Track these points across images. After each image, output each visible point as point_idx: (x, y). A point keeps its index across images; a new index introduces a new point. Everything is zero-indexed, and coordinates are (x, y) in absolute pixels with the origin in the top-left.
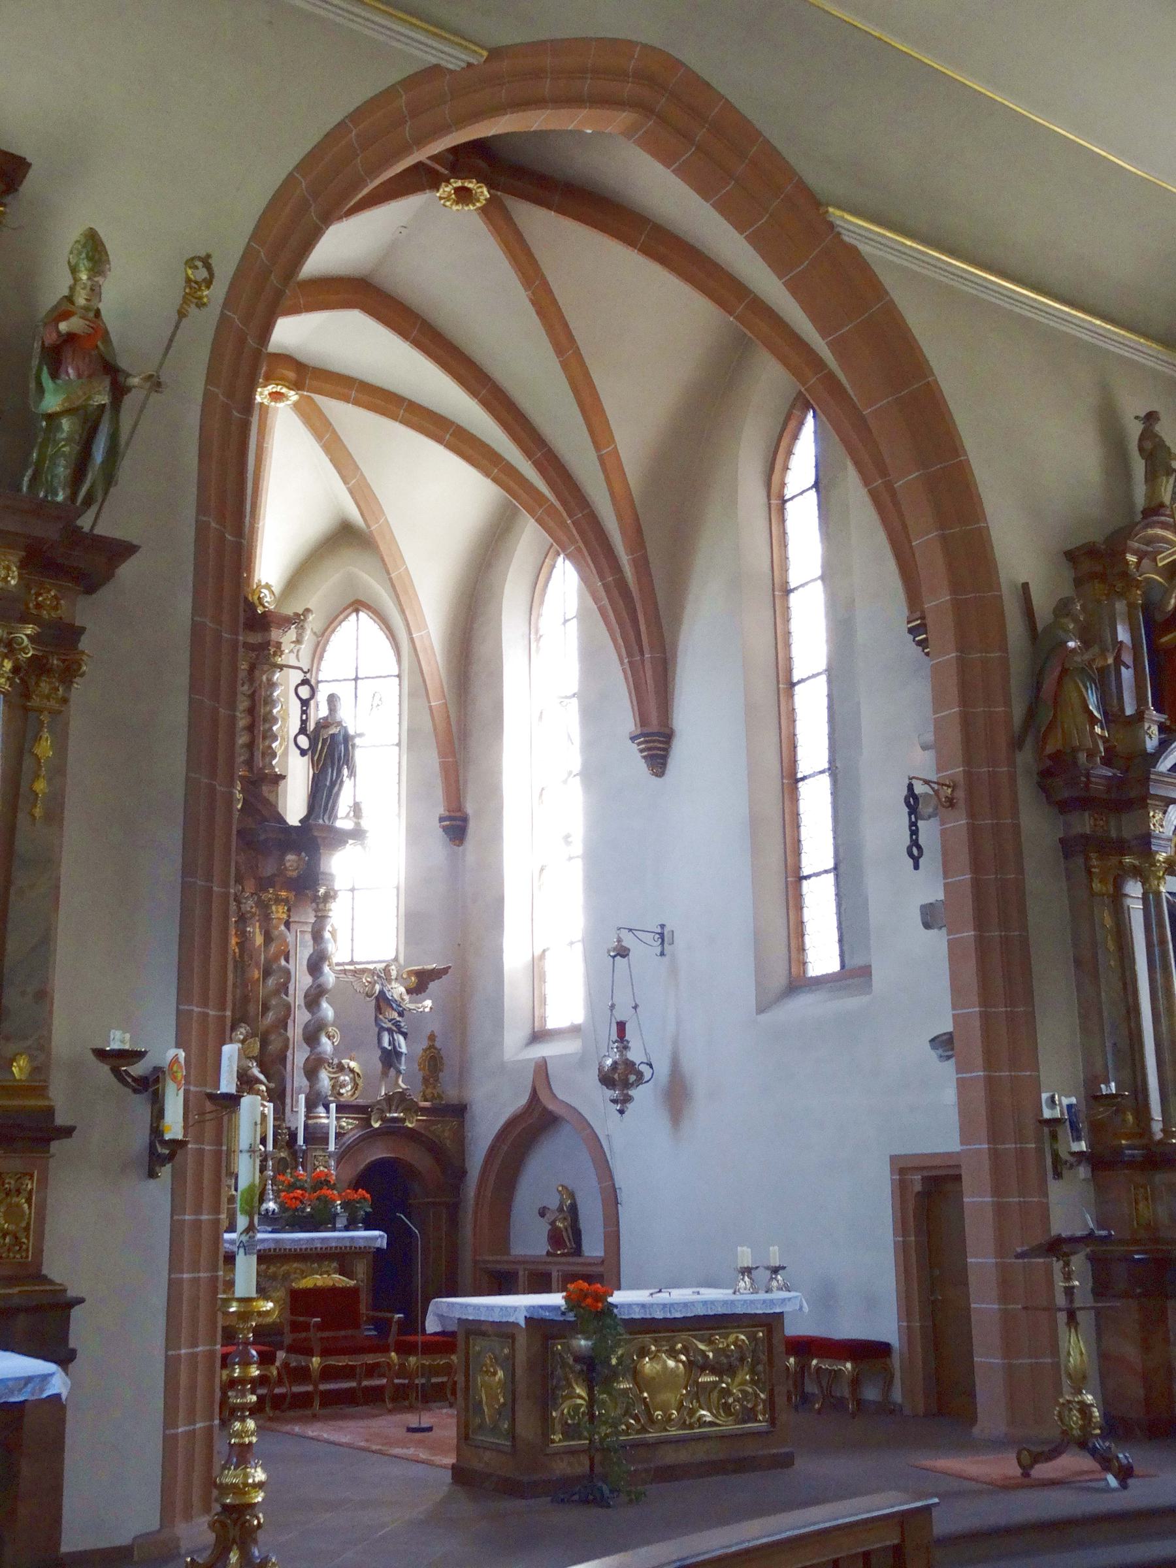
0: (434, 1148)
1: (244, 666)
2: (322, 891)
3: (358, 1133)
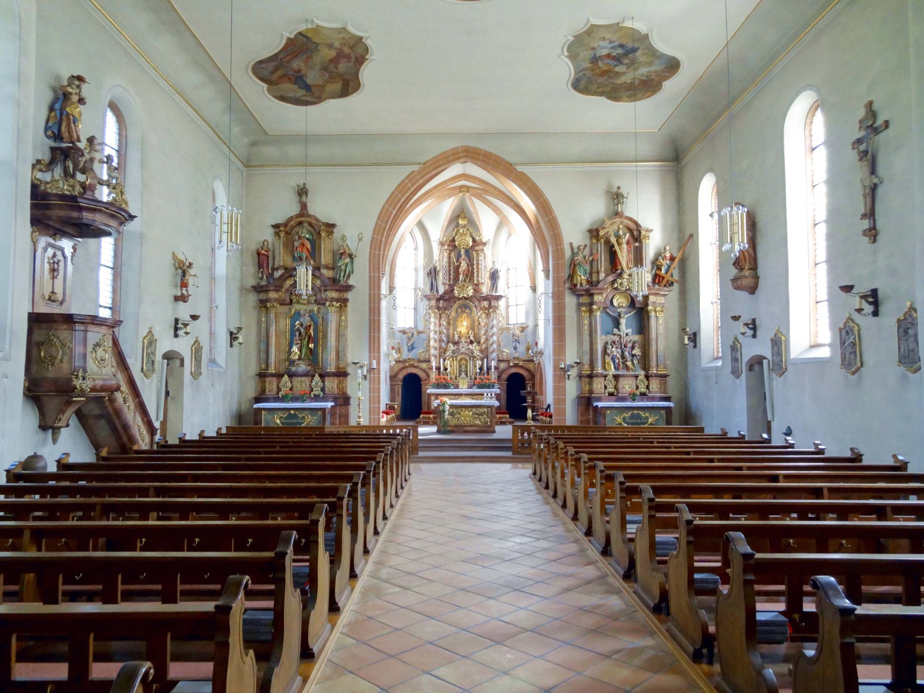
0: (528, 370)
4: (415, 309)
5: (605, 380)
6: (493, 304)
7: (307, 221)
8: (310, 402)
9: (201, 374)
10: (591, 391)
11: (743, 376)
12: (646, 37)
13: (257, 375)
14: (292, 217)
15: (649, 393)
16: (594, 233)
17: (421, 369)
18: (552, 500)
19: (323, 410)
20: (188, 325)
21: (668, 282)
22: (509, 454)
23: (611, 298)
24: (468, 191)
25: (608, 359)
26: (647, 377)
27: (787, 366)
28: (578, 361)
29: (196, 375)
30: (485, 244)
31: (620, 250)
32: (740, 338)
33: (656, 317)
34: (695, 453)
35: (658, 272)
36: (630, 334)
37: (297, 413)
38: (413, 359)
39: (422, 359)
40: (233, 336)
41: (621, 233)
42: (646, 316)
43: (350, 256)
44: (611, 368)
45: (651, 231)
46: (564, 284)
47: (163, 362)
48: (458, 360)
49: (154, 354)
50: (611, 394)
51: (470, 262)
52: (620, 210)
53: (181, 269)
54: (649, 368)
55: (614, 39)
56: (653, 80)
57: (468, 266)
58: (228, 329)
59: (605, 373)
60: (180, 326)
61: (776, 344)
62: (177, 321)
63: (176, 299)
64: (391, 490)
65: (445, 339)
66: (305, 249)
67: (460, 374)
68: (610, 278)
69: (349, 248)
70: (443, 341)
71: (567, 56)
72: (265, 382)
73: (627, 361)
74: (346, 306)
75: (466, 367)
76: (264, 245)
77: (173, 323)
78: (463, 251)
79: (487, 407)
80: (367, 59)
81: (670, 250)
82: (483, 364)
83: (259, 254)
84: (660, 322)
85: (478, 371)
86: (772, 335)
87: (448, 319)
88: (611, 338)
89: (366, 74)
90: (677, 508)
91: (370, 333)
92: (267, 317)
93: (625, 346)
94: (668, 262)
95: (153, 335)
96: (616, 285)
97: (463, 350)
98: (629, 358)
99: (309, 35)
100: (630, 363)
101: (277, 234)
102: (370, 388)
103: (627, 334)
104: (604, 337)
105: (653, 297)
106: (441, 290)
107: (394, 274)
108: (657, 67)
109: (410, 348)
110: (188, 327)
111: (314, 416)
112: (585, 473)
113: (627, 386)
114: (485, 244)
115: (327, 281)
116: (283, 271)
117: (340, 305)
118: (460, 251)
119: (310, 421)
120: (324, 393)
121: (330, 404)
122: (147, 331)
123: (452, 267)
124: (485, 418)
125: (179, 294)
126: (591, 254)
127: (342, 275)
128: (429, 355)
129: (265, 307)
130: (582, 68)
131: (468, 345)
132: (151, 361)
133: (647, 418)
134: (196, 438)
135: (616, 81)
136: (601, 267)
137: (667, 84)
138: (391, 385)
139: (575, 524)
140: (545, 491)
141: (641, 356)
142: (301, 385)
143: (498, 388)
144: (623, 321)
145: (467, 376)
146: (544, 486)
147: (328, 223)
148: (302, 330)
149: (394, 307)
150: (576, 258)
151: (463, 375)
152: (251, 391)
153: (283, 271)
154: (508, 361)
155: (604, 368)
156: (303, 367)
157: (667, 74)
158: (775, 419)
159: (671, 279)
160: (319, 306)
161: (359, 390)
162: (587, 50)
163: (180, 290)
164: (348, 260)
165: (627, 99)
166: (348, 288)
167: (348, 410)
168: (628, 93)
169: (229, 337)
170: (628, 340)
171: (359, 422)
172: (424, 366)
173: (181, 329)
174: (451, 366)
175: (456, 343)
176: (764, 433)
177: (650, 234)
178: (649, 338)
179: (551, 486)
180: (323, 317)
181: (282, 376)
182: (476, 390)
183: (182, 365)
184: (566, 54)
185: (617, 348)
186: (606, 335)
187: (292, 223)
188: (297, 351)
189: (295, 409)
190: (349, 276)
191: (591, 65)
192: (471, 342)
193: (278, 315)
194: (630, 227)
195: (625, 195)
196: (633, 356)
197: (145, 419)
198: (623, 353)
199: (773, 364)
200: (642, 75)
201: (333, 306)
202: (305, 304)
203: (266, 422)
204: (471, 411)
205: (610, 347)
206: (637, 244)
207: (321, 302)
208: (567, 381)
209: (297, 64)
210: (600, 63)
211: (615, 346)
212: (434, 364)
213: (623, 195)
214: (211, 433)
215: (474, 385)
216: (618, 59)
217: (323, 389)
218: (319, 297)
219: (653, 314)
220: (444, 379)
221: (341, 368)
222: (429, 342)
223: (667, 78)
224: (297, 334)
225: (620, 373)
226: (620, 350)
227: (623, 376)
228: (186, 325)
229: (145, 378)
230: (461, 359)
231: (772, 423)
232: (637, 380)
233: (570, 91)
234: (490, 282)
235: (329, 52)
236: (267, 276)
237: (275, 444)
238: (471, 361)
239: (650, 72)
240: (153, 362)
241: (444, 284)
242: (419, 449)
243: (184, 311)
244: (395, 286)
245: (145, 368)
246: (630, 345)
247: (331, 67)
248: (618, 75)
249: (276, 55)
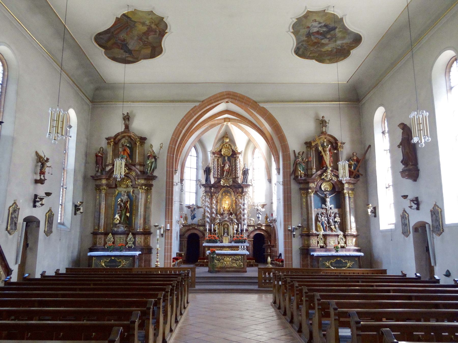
1: (234, 160)
2: (244, 194)
3: (253, 229)
4: (196, 193)
5: (318, 238)
6: (244, 190)
7: (128, 136)
8: (126, 251)
9: (52, 232)
10: (309, 245)
11: (411, 235)
12: (342, 19)
13: (91, 233)
14: (119, 133)
15: (347, 246)
16: (308, 144)
17: (199, 231)
18: (289, 325)
19: (133, 257)
20: (43, 199)
21: (355, 175)
22: (256, 287)
24: (229, 121)
25: (319, 224)
26: (345, 236)
27: (444, 229)
28: (300, 225)
29: (48, 233)
30: (240, 153)
31: (325, 155)
32: (408, 210)
34: (395, 291)
36: (333, 208)
37: (116, 259)
38: (194, 224)
39: (200, 224)
40: (77, 208)
41: (325, 144)
43: (155, 157)
44: (321, 230)
45: (344, 143)
47: (23, 224)
48: (222, 225)
49: (17, 218)
50: (322, 247)
51: (230, 164)
52: (324, 130)
53: (41, 162)
54: (346, 230)
55: (322, 21)
56: (344, 49)
57: (229, 167)
58: (73, 203)
59: (318, 233)
60: (38, 200)
61: (435, 214)
62: (36, 196)
63: (36, 182)
64: (171, 318)
65: (215, 212)
66: (125, 153)
67: (224, 234)
68: (319, 172)
69: (154, 152)
70: (213, 213)
71: (292, 32)
72: (96, 238)
73: (331, 225)
74: (151, 189)
75: (228, 229)
76: (100, 150)
77: (33, 197)
78: (226, 158)
79: (241, 255)
80: (167, 33)
81: (356, 155)
82: (238, 227)
83: (97, 156)
84: (352, 201)
85: (235, 232)
86: (431, 208)
87: (217, 199)
88: (321, 211)
89: (166, 42)
90: (382, 332)
91: (166, 206)
92: (100, 196)
93: (330, 216)
95: (17, 206)
96: (323, 177)
97: (226, 219)
98: (333, 224)
99: (130, 16)
100: (334, 227)
101: (109, 143)
102: (165, 242)
103: (331, 208)
104: (316, 209)
106: (213, 181)
107: (183, 171)
108: (347, 41)
109: (193, 217)
110: (44, 200)
111: (127, 261)
112: (318, 309)
113: (332, 242)
114: (240, 153)
115: (139, 173)
116: (112, 167)
117: (147, 188)
118: (224, 157)
119: (124, 263)
120: (135, 245)
121: (138, 253)
122: (13, 202)
123: (219, 168)
124: (240, 263)
125: (39, 178)
126: (307, 158)
127: (149, 169)
128: (205, 222)
129: (99, 189)
130: (301, 40)
131: (229, 216)
132: (14, 223)
133: (346, 263)
134: (54, 274)
135: (321, 49)
136: (313, 165)
137: (353, 52)
138: (180, 240)
139: (300, 336)
140: (283, 317)
141: (340, 222)
142: (120, 240)
143: (248, 243)
144: (328, 200)
145: (228, 235)
146: (283, 313)
147: (141, 137)
148: (122, 204)
149: (182, 190)
150: (297, 160)
151: (226, 234)
152: (88, 244)
153: (112, 167)
154: (253, 226)
155: (316, 230)
156: (122, 229)
157: (354, 45)
158: (437, 264)
159: (358, 173)
160: (134, 189)
161: (158, 244)
162: (304, 28)
163: (39, 176)
164: (153, 160)
165: (328, 62)
166: (154, 178)
167: (150, 257)
168: (329, 58)
169: (74, 208)
170: (332, 212)
171: (157, 265)
172: (202, 228)
173: (38, 202)
174: (218, 229)
175: (222, 214)
176: (417, 273)
177: (344, 145)
178: (345, 211)
179: (288, 313)
180: (136, 196)
181: (108, 234)
182: (233, 244)
183: (38, 226)
184: (292, 30)
185: (324, 217)
186: (317, 209)
187: (119, 137)
188: (118, 218)
189: (115, 256)
190: (154, 170)
191: (306, 38)
192: (231, 214)
193: (107, 194)
194: (331, 141)
195: (327, 121)
196: (335, 222)
197: (3, 263)
198: (328, 220)
199: (433, 226)
200: (339, 46)
201: (142, 189)
202: (124, 188)
203: (96, 265)
204: (231, 258)
205: (320, 216)
206: (335, 151)
207: (136, 186)
208: (293, 238)
209: (123, 35)
210: (312, 37)
211: (323, 216)
212: (208, 227)
213: (326, 122)
214: (63, 271)
215: (233, 241)
216: (324, 35)
217: (134, 243)
218: (134, 183)
219: (347, 195)
220: (214, 237)
221: (147, 229)
222: (205, 213)
223: (353, 48)
224: (119, 207)
225: (328, 233)
226: (327, 219)
227: (329, 235)
228: (41, 199)
229: (9, 234)
230: (225, 225)
231: (435, 267)
232: (338, 237)
233: (293, 56)
234: (242, 177)
235: (143, 27)
236: (101, 170)
237: (90, 282)
238: (231, 226)
239: (343, 43)
240: (16, 224)
241: (214, 177)
242: (196, 284)
243: (41, 190)
244: (184, 179)
245: (9, 227)
246: (333, 215)
247: (144, 38)
248: (323, 45)
249: (109, 29)
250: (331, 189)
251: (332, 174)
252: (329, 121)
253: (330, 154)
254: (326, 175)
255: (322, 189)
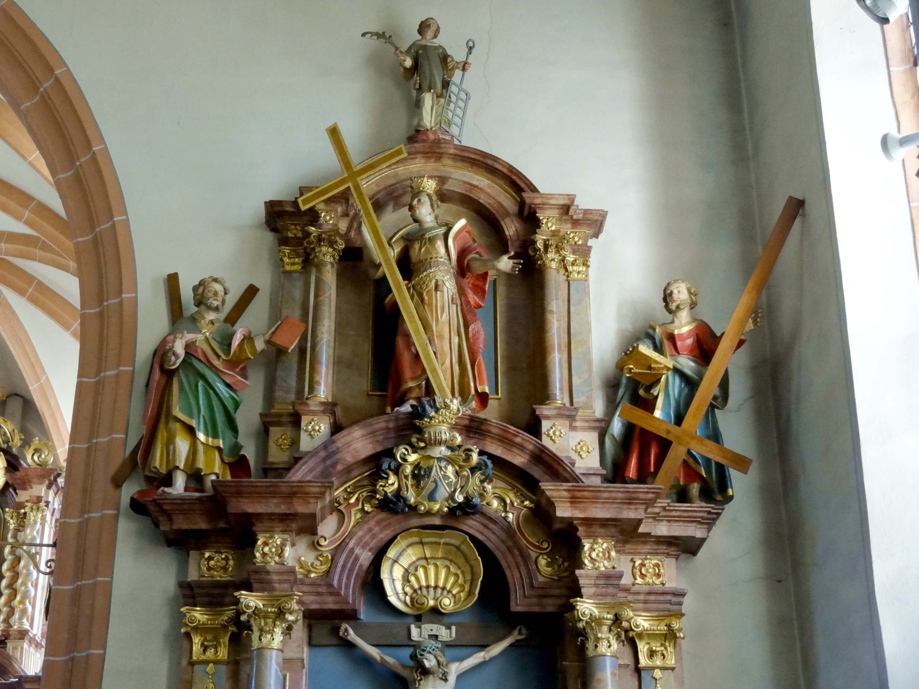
23: (365, 557)
33: (638, 670)
35: (639, 417)
42: (570, 665)
46: (117, 483)
94: (687, 364)
105: (602, 545)
194: (483, 199)
195: (457, 54)
213: (444, 58)
250: (470, 593)
251: (475, 457)
252: (470, 49)
253: (461, 291)
254: (417, 466)
255: (393, 599)
